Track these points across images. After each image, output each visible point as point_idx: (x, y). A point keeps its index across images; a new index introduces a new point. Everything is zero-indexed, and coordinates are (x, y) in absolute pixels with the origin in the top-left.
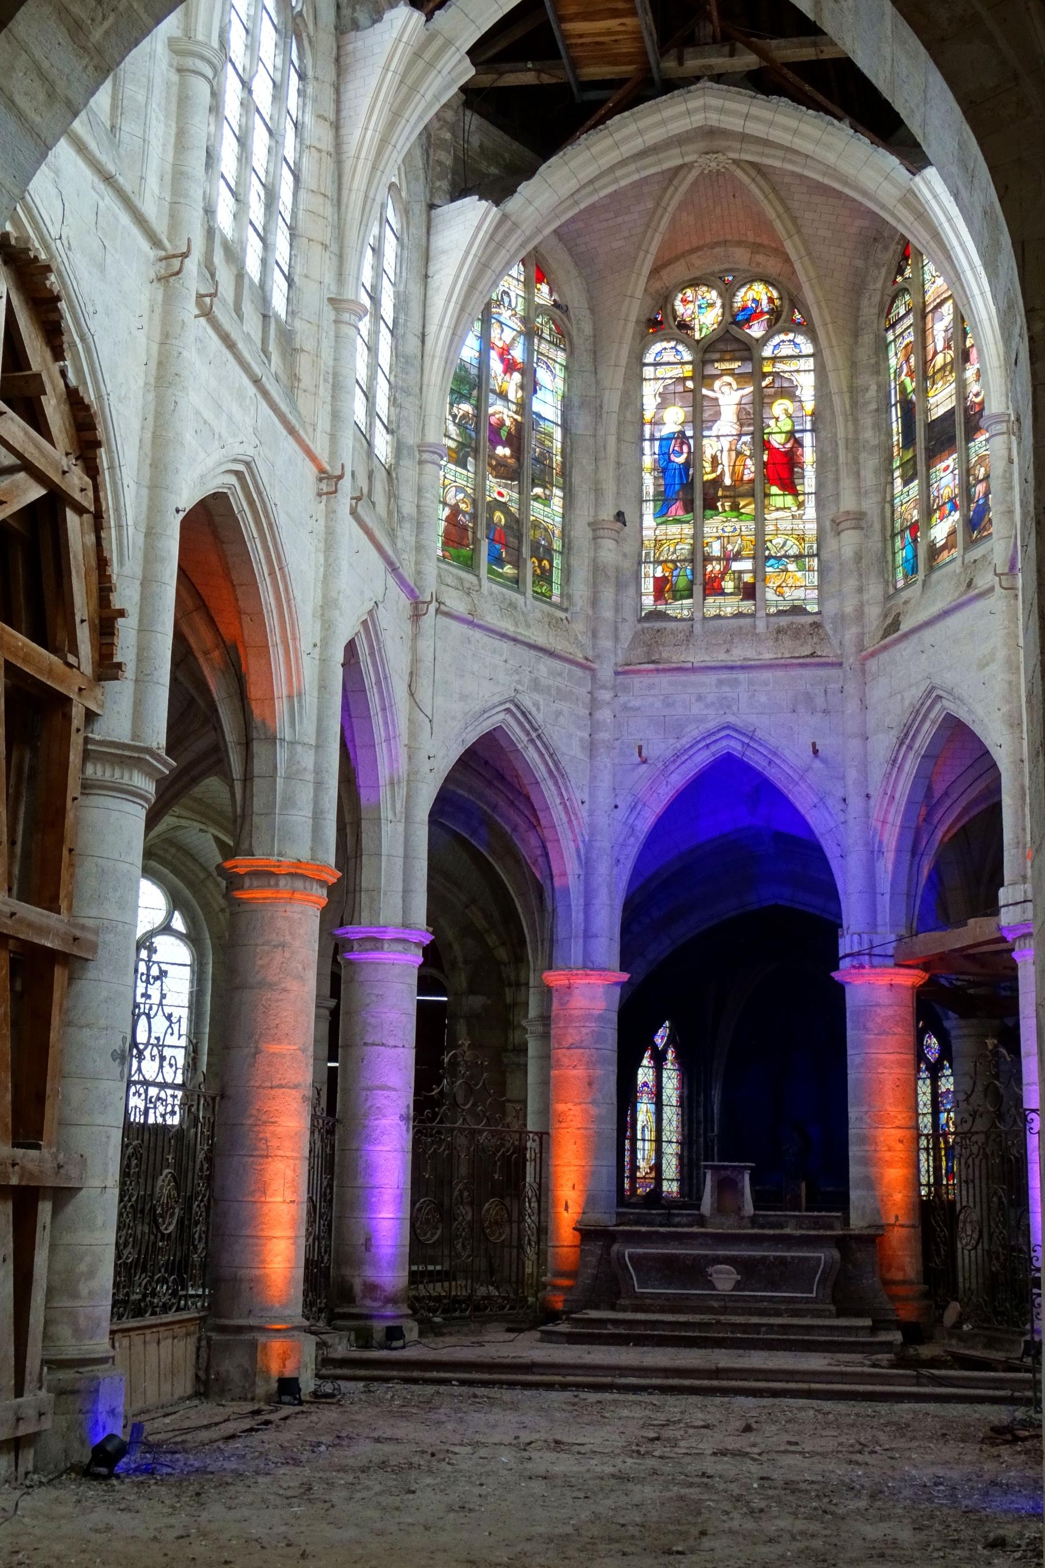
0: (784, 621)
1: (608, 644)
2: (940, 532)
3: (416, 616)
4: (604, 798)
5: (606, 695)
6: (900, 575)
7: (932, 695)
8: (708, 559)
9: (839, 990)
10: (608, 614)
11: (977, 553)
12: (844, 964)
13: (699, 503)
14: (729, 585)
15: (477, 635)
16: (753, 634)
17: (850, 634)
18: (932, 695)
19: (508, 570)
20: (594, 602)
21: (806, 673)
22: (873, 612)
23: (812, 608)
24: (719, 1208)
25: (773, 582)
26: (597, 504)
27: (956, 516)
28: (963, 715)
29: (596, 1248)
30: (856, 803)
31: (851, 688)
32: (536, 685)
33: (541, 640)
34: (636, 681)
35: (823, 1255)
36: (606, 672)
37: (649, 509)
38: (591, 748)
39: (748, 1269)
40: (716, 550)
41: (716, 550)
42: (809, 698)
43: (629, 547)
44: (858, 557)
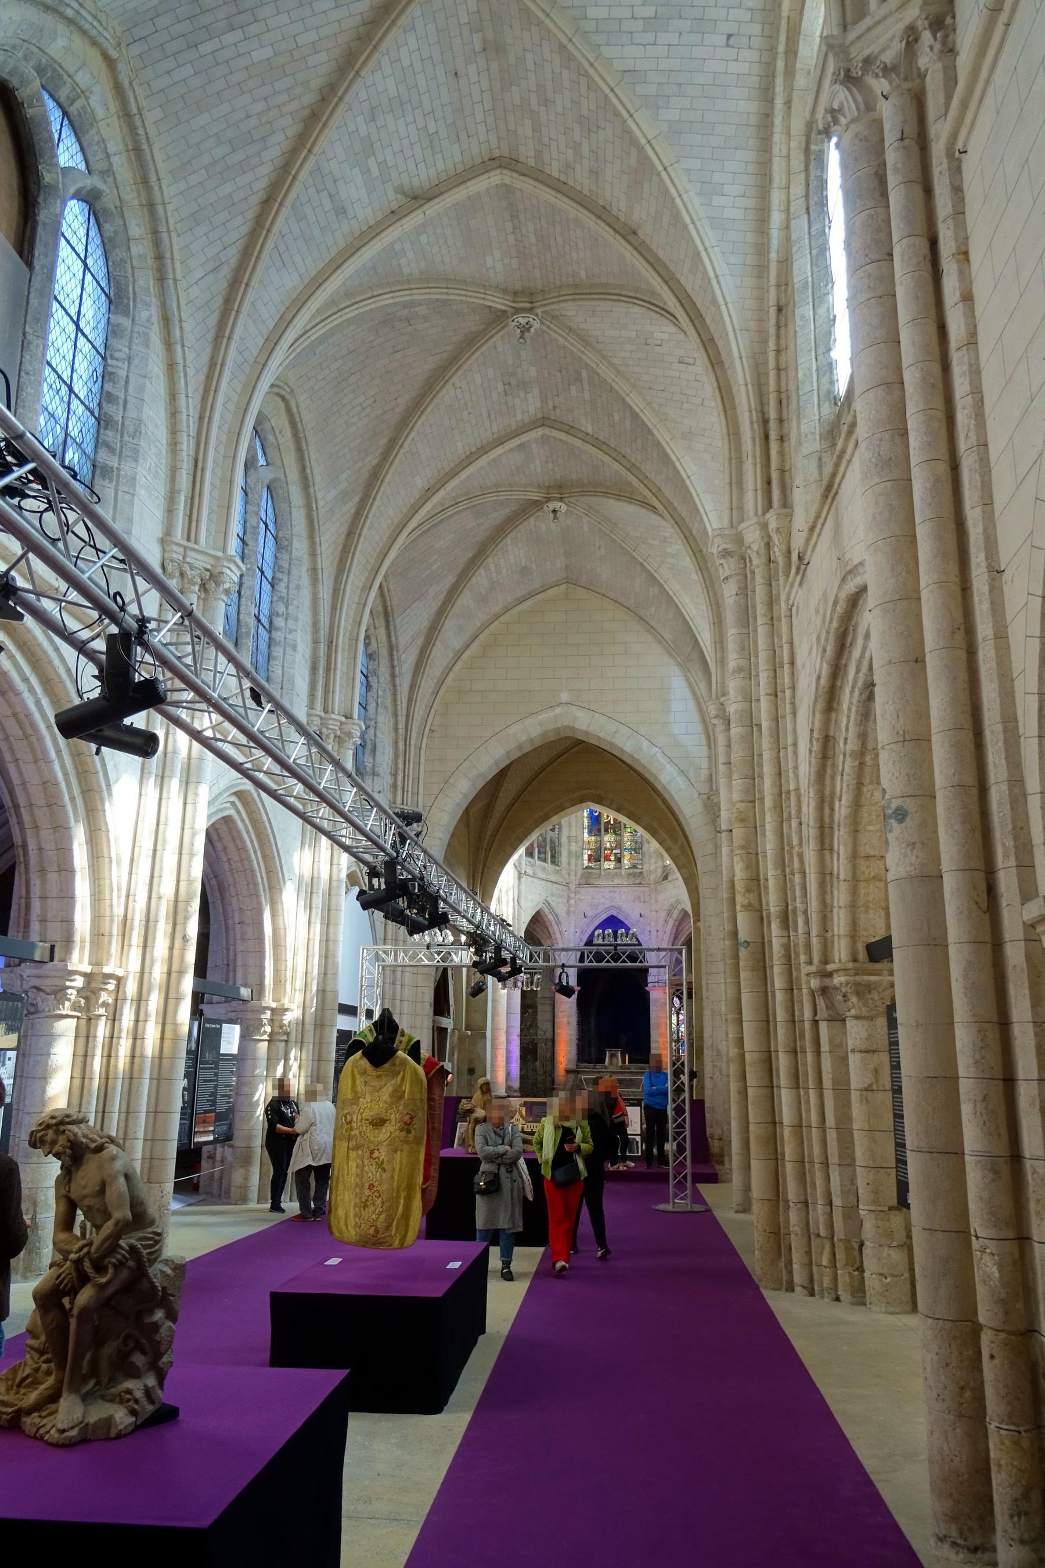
0: (631, 871)
1: (573, 878)
3: (519, 878)
4: (572, 930)
5: (572, 895)
8: (605, 849)
9: (648, 993)
10: (573, 867)
12: (650, 985)
13: (603, 830)
15: (535, 880)
16: (619, 875)
17: (653, 877)
19: (542, 856)
20: (569, 863)
22: (660, 870)
24: (611, 1063)
26: (570, 830)
29: (572, 1076)
30: (654, 932)
31: (653, 895)
32: (552, 895)
33: (553, 879)
34: (583, 890)
36: (573, 887)
37: (586, 831)
38: (568, 913)
42: (639, 898)
43: (580, 844)
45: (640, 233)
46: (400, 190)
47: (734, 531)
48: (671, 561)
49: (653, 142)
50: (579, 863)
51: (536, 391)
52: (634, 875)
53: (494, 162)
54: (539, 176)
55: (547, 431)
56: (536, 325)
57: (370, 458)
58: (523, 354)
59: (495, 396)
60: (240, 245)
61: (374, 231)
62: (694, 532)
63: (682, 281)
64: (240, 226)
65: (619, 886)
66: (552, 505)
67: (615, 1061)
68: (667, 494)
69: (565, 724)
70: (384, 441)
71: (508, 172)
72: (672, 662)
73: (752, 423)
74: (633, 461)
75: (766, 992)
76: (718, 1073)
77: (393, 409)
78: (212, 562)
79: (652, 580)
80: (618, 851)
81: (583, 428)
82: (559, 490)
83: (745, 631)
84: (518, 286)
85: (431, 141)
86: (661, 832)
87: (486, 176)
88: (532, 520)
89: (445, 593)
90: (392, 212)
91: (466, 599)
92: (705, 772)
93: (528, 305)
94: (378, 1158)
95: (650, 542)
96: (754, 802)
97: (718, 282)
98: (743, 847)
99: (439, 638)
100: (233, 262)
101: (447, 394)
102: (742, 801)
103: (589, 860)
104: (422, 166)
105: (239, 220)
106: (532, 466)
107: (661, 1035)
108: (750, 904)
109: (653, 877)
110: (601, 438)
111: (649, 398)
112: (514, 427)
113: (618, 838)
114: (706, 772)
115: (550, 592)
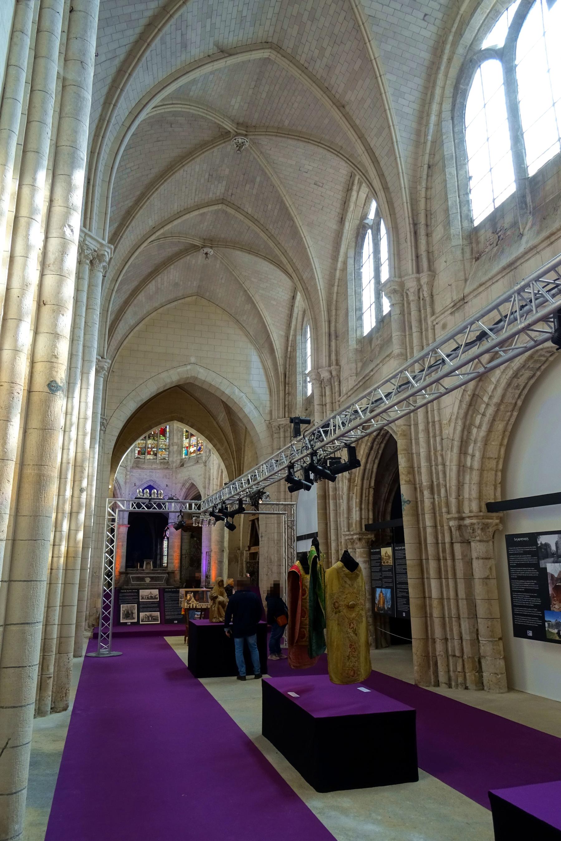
0: (162, 461)
1: (129, 463)
2: (192, 449)
4: (127, 493)
6: (184, 455)
7: (189, 479)
8: (148, 448)
11: (199, 456)
14: (152, 453)
17: (175, 465)
18: (189, 479)
21: (166, 471)
22: (179, 461)
23: (167, 459)
24: (146, 568)
25: (160, 453)
27: (195, 448)
28: (195, 483)
29: (123, 576)
31: (174, 474)
34: (135, 471)
35: (165, 576)
36: (129, 468)
38: (125, 483)
39: (152, 578)
40: (150, 446)
41: (150, 446)
42: (166, 476)
44: (176, 451)
45: (347, 108)
46: (216, 44)
47: (399, 280)
48: (261, 291)
49: (377, 59)
50: (133, 455)
51: (224, 183)
52: (164, 463)
53: (267, 44)
54: (292, 59)
55: (224, 207)
56: (247, 144)
57: (126, 203)
58: (226, 161)
59: (202, 181)
60: (128, 48)
61: (198, 64)
62: (304, 277)
63: (369, 139)
64: (132, 35)
65: (155, 469)
66: (206, 250)
67: (147, 566)
68: (290, 254)
69: (193, 375)
70: (138, 193)
71: (275, 53)
72: (253, 347)
73: (409, 224)
74: (272, 233)
75: (419, 528)
76: (270, 572)
77: (147, 175)
78: (98, 246)
79: (250, 300)
80: (155, 449)
81: (246, 210)
82: (210, 242)
83: (403, 334)
84: (241, 120)
85: (242, 21)
86: (215, 440)
87: (263, 51)
88: (188, 257)
89: (131, 290)
90: (209, 56)
91: (141, 297)
92: (268, 409)
93: (244, 132)
94: (353, 628)
95: (253, 279)
96: (410, 426)
97: (397, 145)
98: (405, 450)
99: (124, 317)
100: (122, 57)
101: (179, 175)
102: (404, 425)
103: (139, 454)
104: (231, 34)
105: (130, 32)
106: (202, 225)
107: (174, 552)
108: (410, 480)
109: (175, 465)
110: (256, 217)
111: (294, 200)
112: (206, 201)
113: (156, 442)
114: (269, 409)
115: (187, 299)
